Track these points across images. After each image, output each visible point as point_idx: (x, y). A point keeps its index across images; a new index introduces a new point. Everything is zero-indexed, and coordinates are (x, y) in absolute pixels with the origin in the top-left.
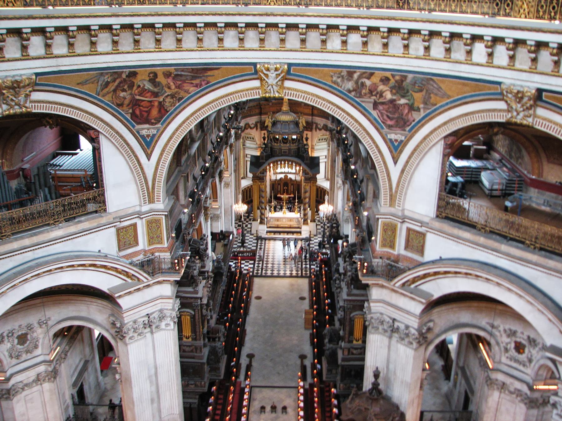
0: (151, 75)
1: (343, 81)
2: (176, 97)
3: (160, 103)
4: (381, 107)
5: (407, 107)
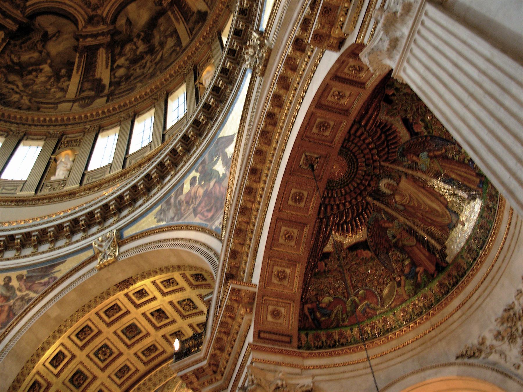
0: (6, 280)
1: (165, 215)
2: (25, 300)
3: (10, 307)
4: (200, 209)
5: (216, 185)
